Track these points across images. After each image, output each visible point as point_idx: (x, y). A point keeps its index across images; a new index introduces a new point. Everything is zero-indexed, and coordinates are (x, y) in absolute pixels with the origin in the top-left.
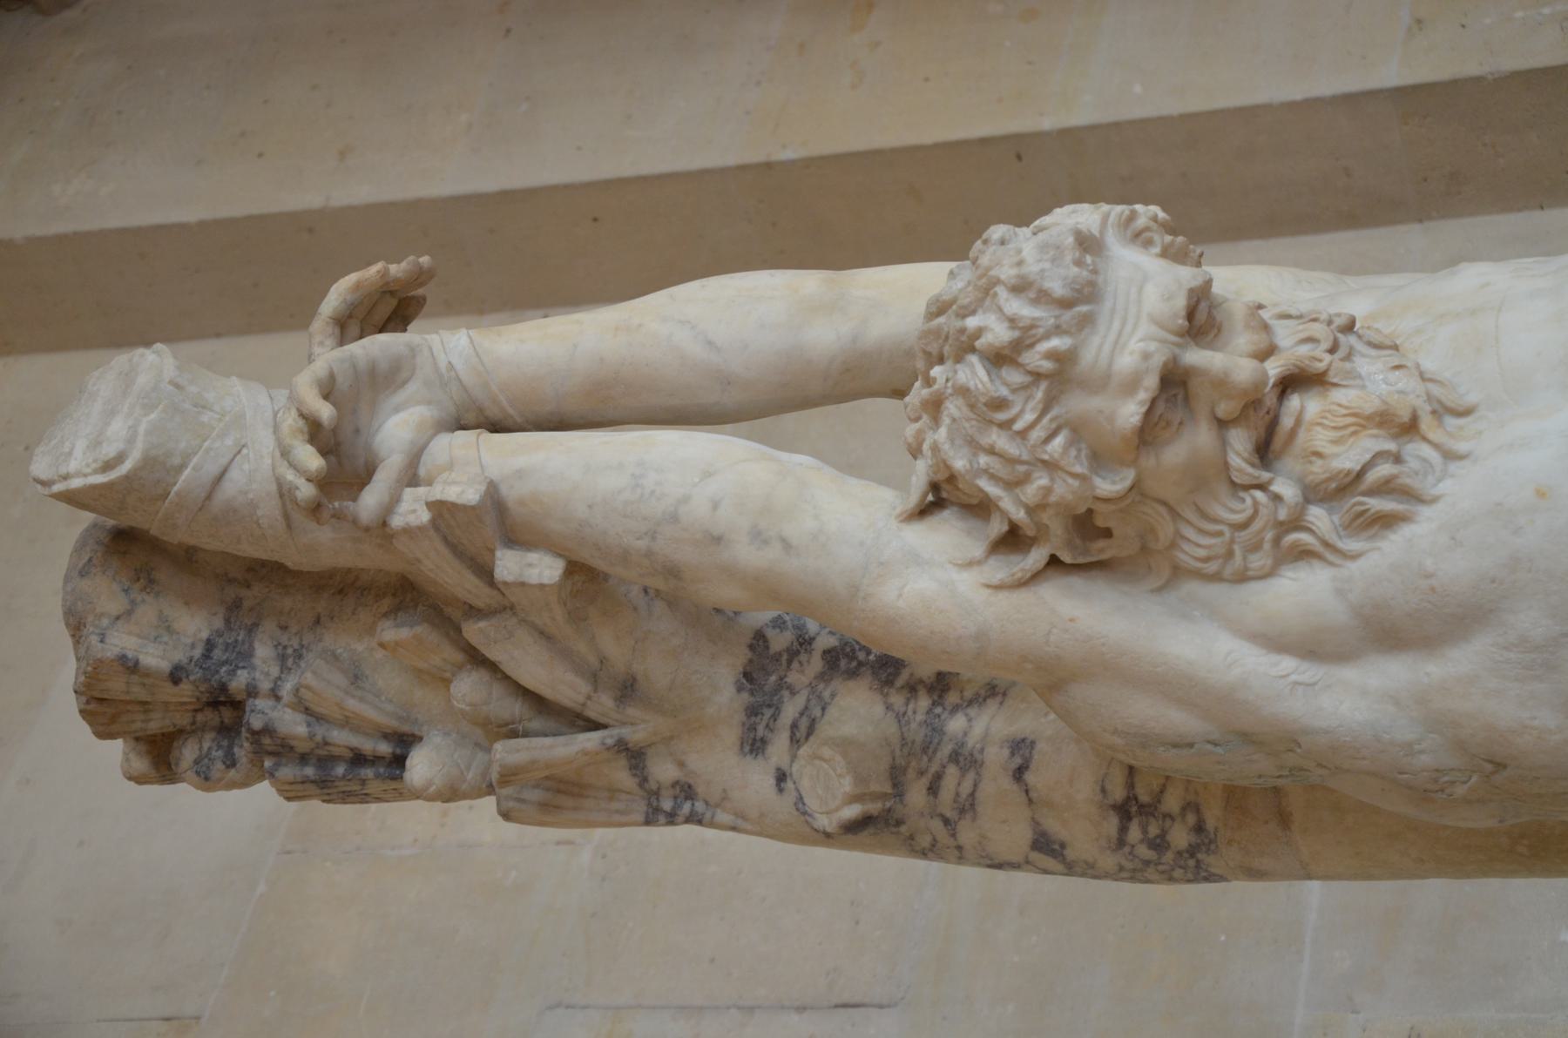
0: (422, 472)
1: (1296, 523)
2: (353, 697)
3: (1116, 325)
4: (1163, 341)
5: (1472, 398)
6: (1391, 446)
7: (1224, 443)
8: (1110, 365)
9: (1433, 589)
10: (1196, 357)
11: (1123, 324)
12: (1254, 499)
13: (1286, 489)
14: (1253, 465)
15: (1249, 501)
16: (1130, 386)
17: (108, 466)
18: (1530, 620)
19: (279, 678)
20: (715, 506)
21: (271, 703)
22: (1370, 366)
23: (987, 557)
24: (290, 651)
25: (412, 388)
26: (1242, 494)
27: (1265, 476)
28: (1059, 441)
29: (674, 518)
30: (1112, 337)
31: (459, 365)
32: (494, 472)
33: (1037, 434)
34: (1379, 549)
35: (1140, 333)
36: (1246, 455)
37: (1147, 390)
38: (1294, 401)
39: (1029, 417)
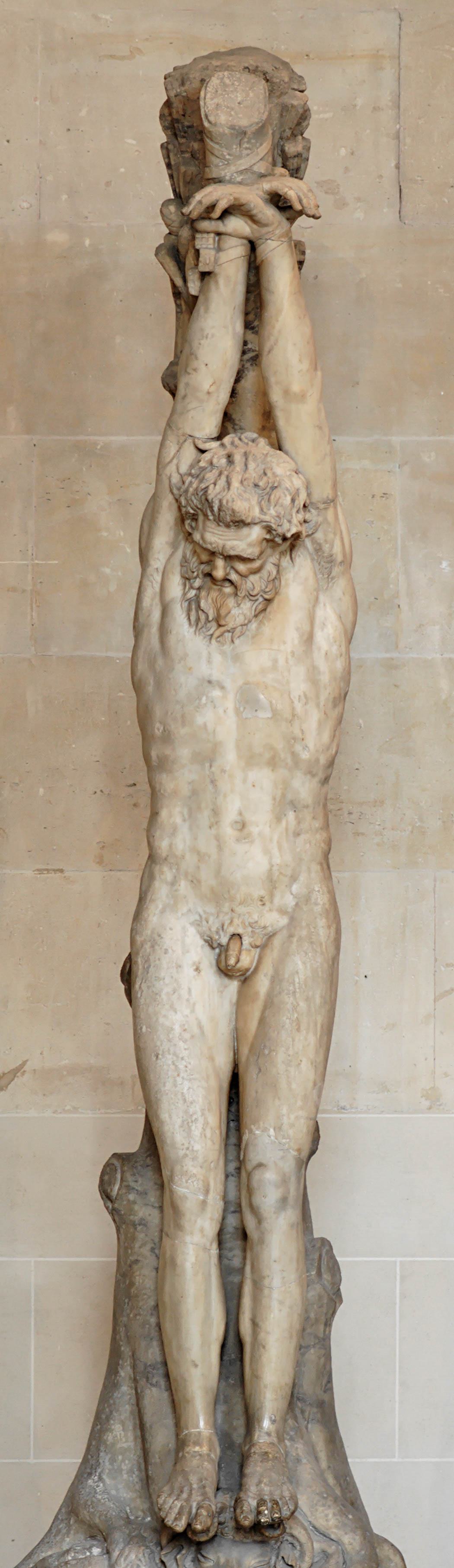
0: (223, 237)
5: (237, 641)
6: (210, 618)
16: (202, 538)
17: (206, 116)
18: (160, 662)
22: (247, 607)
25: (255, 226)
28: (192, 511)
38: (227, 584)
39: (195, 501)
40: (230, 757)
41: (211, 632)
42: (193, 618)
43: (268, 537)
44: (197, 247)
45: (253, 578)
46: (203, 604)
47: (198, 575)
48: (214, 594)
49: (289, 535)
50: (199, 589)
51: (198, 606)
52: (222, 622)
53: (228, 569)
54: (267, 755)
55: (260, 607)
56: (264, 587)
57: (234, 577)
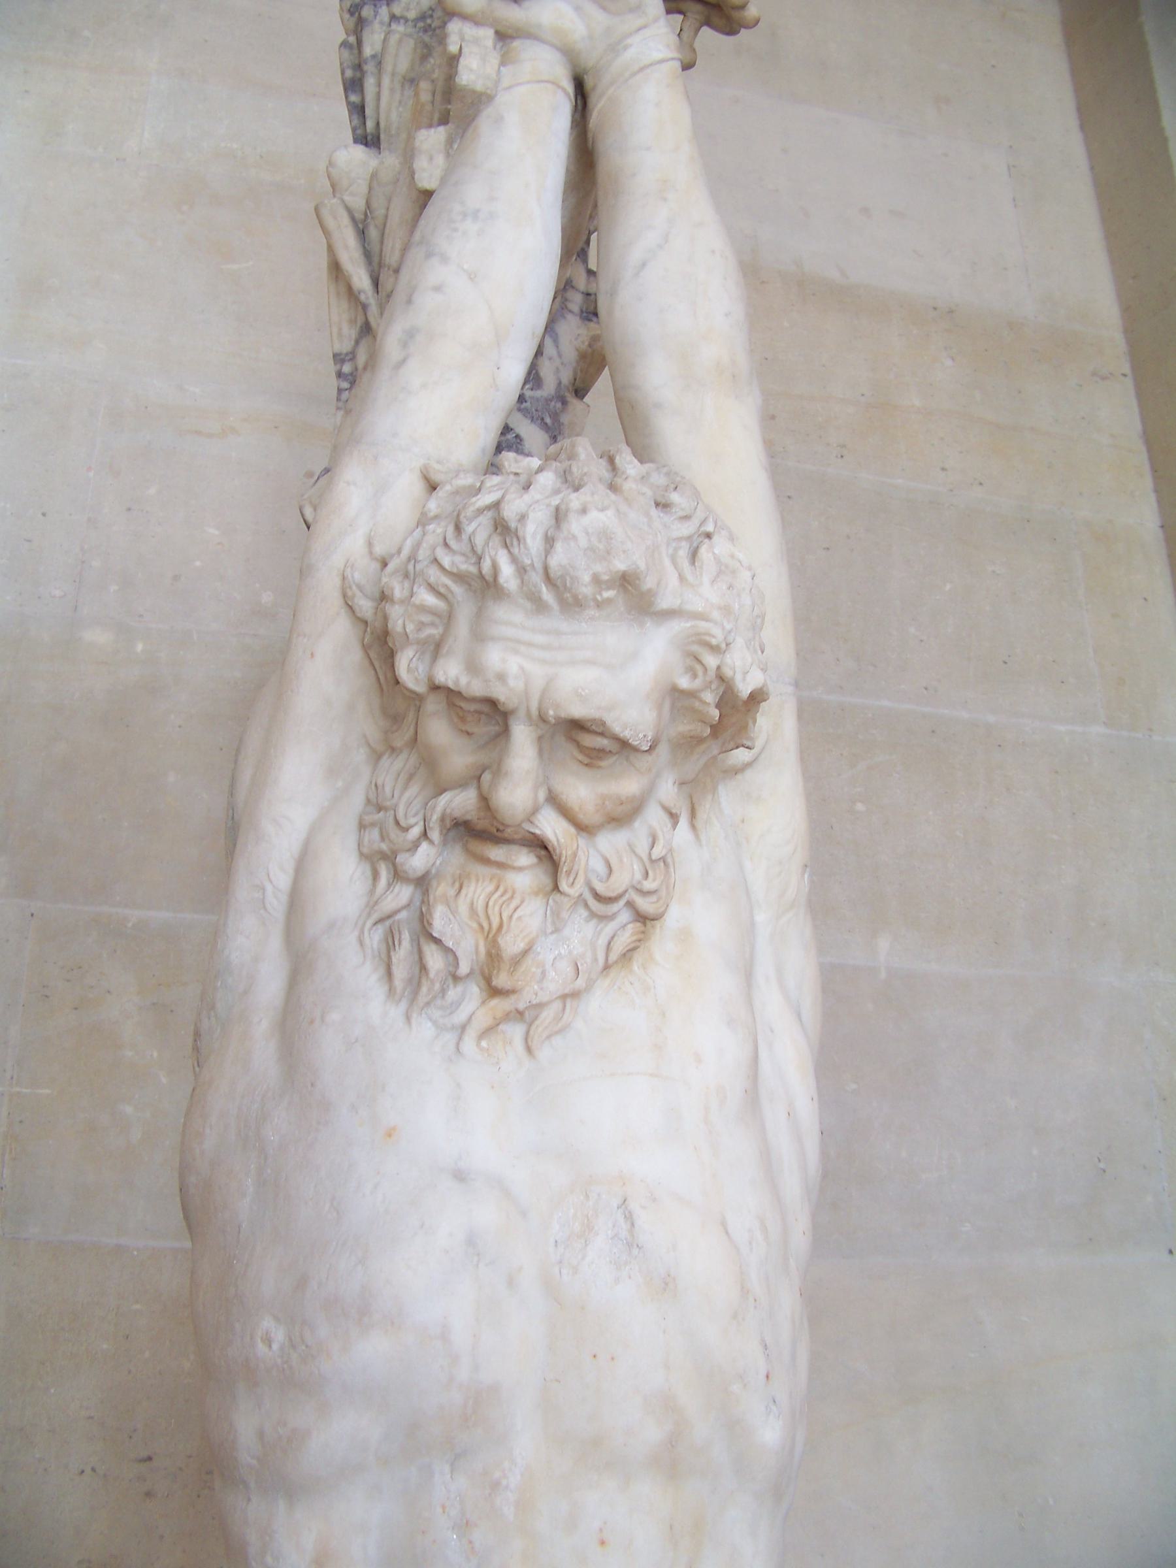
0: (516, 44)
1: (398, 875)
2: (392, 81)
3: (540, 639)
4: (526, 692)
5: (545, 1053)
7: (462, 784)
8: (493, 639)
9: (312, 1022)
10: (522, 737)
11: (543, 647)
12: (416, 824)
13: (419, 860)
14: (442, 819)
15: (412, 821)
16: (473, 667)
19: (407, 20)
20: (438, 289)
21: (386, 19)
22: (581, 936)
23: (376, 559)
24: (429, 21)
26: (421, 816)
27: (435, 835)
28: (430, 600)
29: (429, 255)
30: (527, 636)
31: (630, 54)
32: (502, 99)
33: (434, 574)
34: (363, 963)
35: (529, 666)
36: (448, 811)
37: (469, 683)
38: (525, 858)
39: (446, 561)
40: (526, 1445)
41: (461, 1016)
42: (400, 973)
43: (684, 683)
44: (453, 48)
45: (610, 842)
46: (440, 922)
47: (425, 835)
48: (478, 891)
49: (744, 689)
50: (423, 882)
51: (425, 933)
52: (502, 980)
53: (542, 795)
54: (653, 1433)
55: (625, 939)
56: (638, 876)
57: (551, 826)
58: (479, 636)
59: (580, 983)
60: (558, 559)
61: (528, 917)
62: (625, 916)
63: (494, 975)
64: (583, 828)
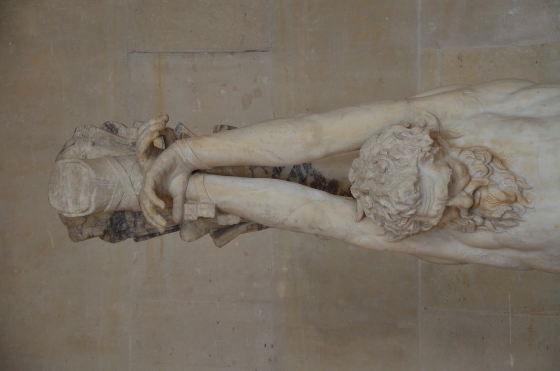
0: (187, 197)
5: (531, 184)
13: (479, 220)
20: (296, 221)
30: (427, 206)
31: (190, 160)
38: (478, 194)
39: (402, 223)
43: (432, 160)
45: (472, 172)
46: (497, 215)
47: (472, 220)
48: (488, 206)
49: (431, 141)
50: (484, 218)
52: (513, 199)
53: (464, 194)
55: (499, 165)
56: (480, 162)
57: (470, 189)
58: (426, 216)
59: (512, 177)
60: (411, 202)
61: (494, 192)
62: (492, 164)
63: (510, 200)
64: (470, 180)
